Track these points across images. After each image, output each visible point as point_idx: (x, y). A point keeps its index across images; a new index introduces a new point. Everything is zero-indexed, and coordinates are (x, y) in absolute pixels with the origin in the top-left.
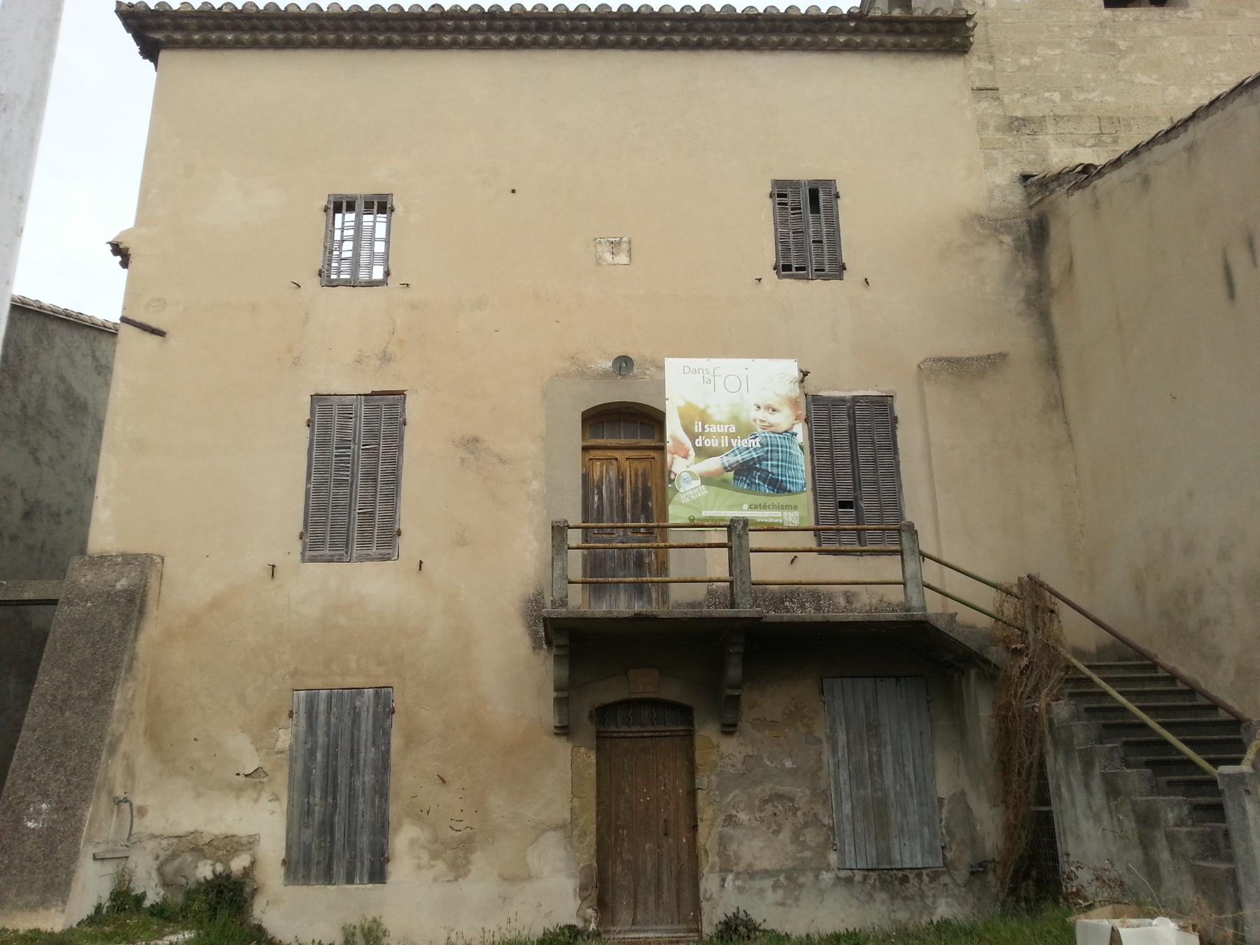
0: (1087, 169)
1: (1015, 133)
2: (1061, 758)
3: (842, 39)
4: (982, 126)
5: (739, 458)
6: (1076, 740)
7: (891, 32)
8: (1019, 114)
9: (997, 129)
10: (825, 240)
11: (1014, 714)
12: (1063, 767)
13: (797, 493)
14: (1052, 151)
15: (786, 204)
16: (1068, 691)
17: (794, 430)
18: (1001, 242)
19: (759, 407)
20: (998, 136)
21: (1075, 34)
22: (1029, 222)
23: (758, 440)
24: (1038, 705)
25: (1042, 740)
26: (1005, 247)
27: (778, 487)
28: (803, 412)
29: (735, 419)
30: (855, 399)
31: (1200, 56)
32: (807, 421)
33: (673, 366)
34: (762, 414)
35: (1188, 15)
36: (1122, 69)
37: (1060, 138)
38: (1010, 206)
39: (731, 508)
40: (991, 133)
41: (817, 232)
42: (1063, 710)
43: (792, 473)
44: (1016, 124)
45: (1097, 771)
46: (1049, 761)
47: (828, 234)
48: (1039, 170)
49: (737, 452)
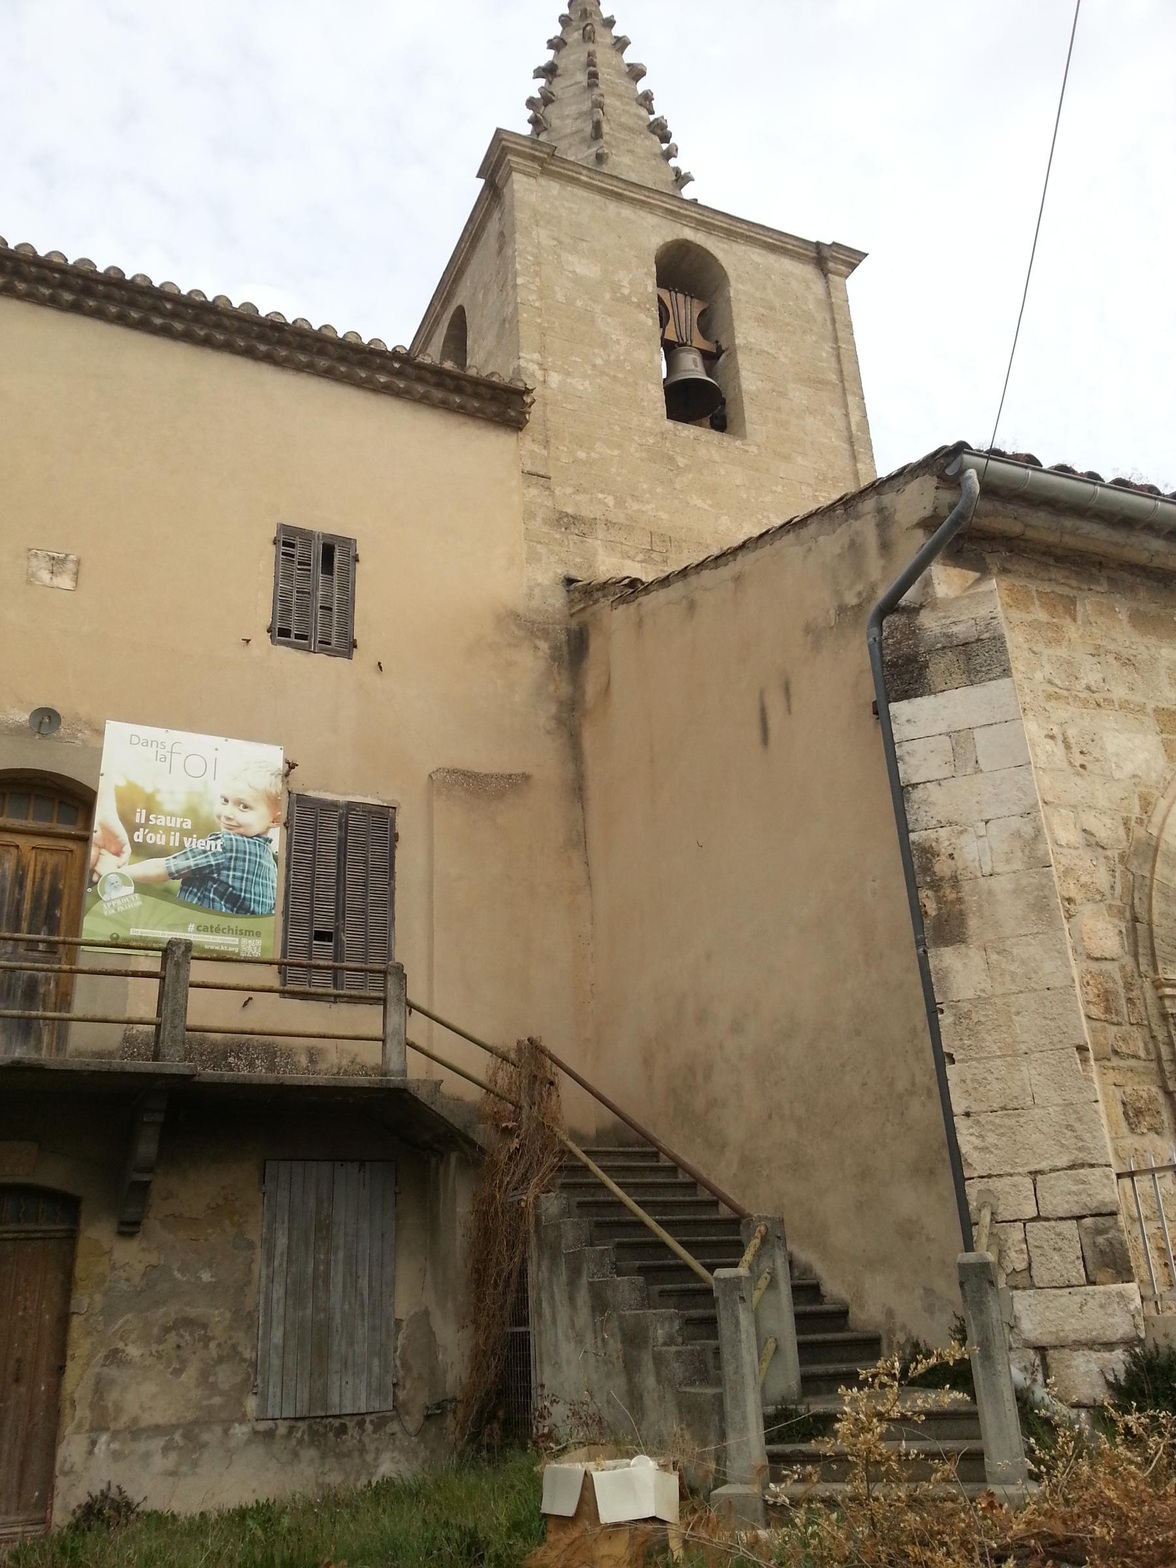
0: (634, 583)
1: (563, 530)
2: (545, 1264)
3: (383, 379)
4: (530, 515)
5: (192, 863)
6: (563, 1241)
7: (440, 385)
8: (570, 510)
9: (545, 521)
10: (335, 608)
11: (496, 1209)
12: (546, 1275)
13: (262, 916)
15: (293, 556)
16: (560, 1181)
17: (269, 835)
18: (536, 648)
19: (226, 801)
20: (545, 529)
22: (568, 631)
23: (219, 842)
24: (525, 1198)
25: (526, 1243)
26: (540, 654)
27: (238, 905)
28: (283, 814)
29: (192, 812)
30: (351, 806)
31: (753, 491)
32: (287, 825)
33: (117, 733)
34: (230, 810)
35: (745, 447)
36: (678, 486)
37: (610, 544)
38: (550, 609)
39: (171, 927)
40: (537, 524)
41: (328, 597)
42: (552, 1204)
43: (259, 889)
44: (565, 520)
45: (584, 1280)
46: (532, 1269)
47: (340, 601)
48: (585, 576)
49: (189, 855)
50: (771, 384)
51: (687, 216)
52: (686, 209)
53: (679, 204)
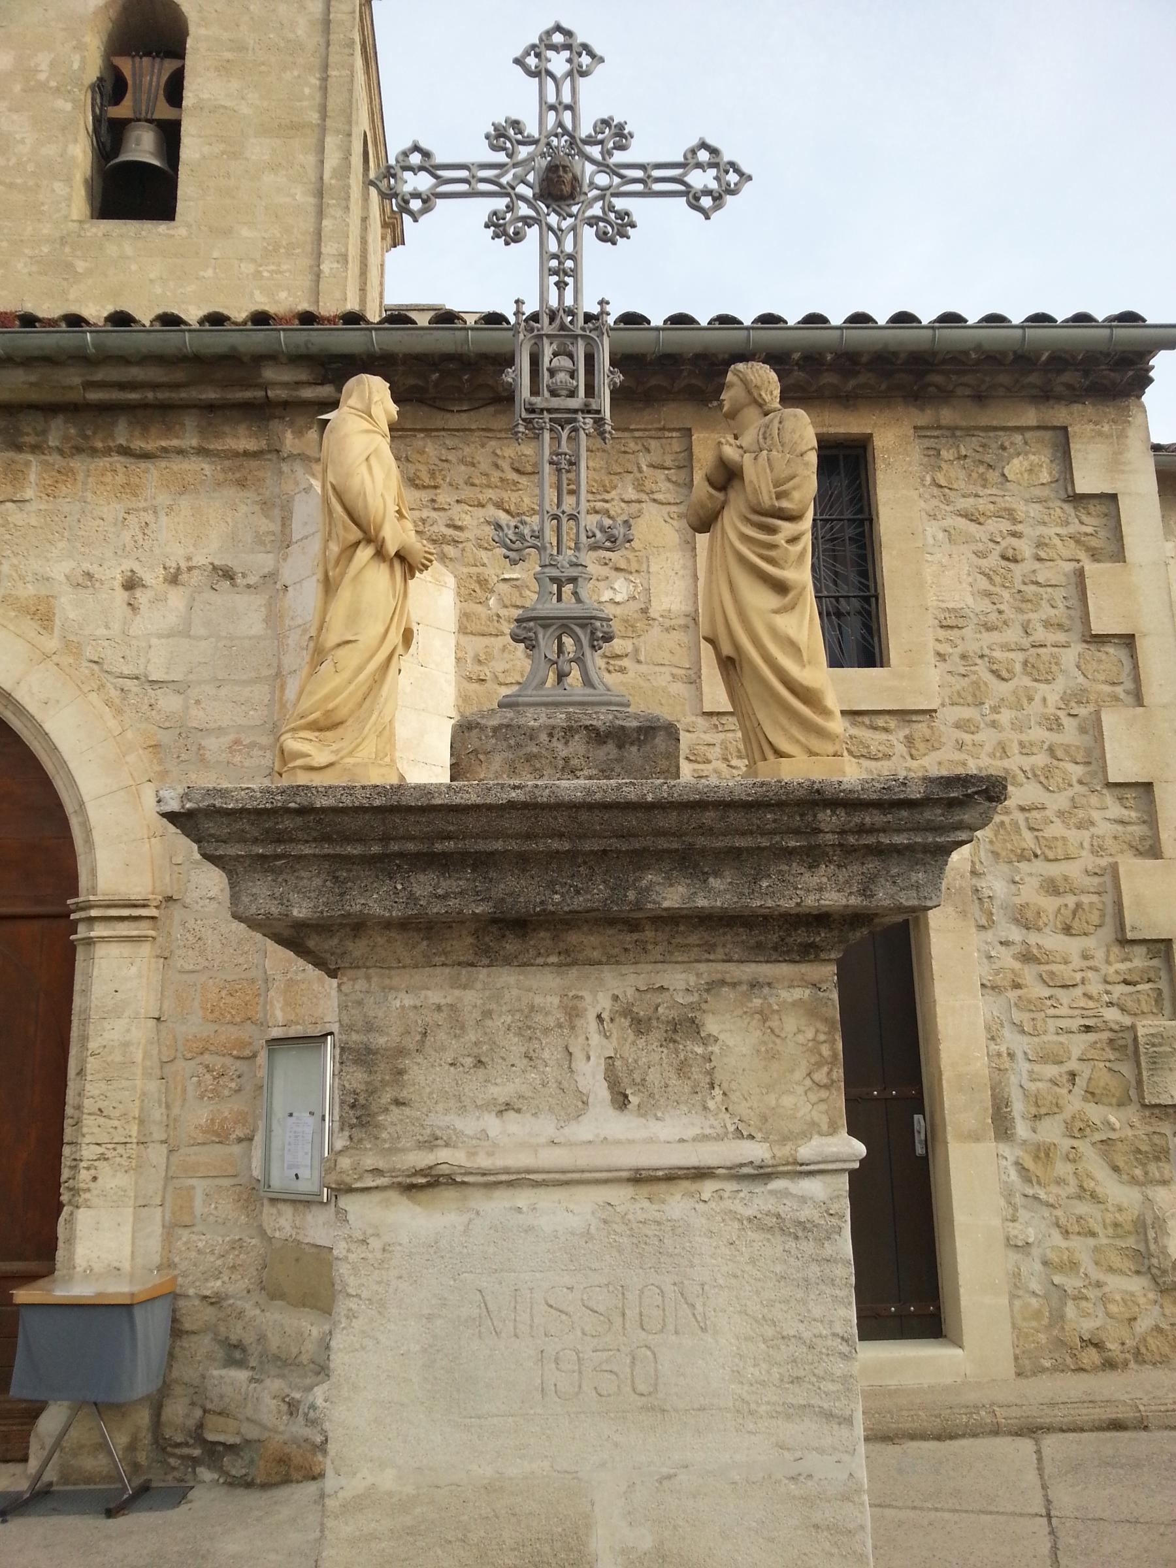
21: (26, 251)
35: (171, 232)
50: (222, 147)
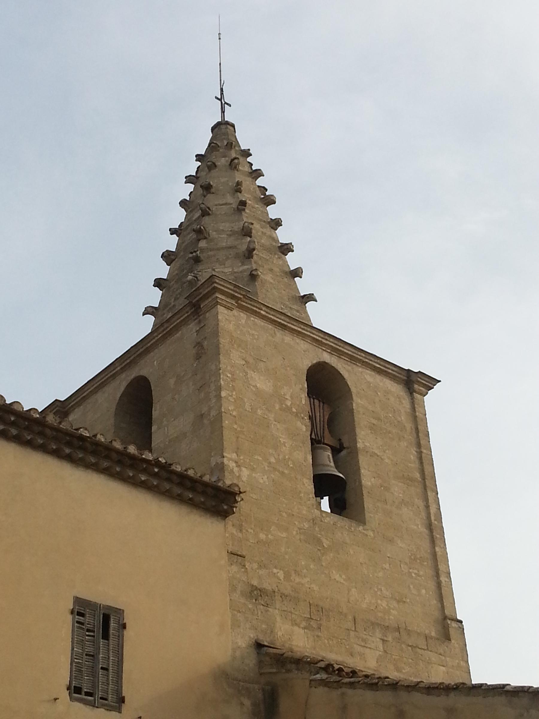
1: (254, 600)
4: (233, 589)
7: (181, 484)
9: (243, 594)
14: (278, 625)
20: (243, 600)
40: (236, 596)
51: (326, 344)
52: (326, 340)
53: (322, 336)
